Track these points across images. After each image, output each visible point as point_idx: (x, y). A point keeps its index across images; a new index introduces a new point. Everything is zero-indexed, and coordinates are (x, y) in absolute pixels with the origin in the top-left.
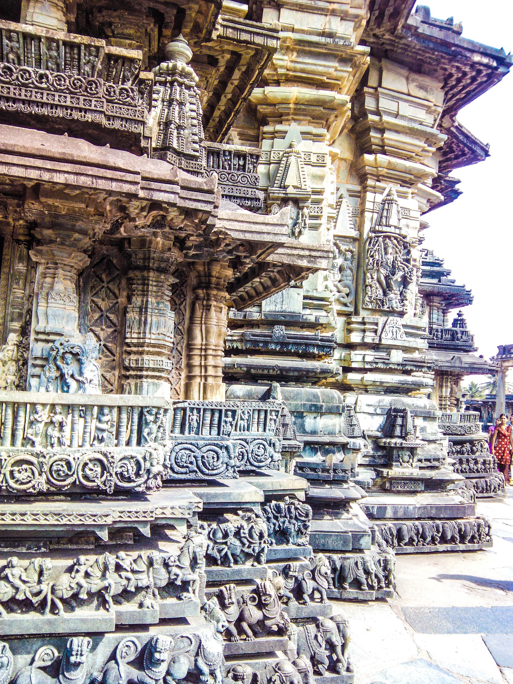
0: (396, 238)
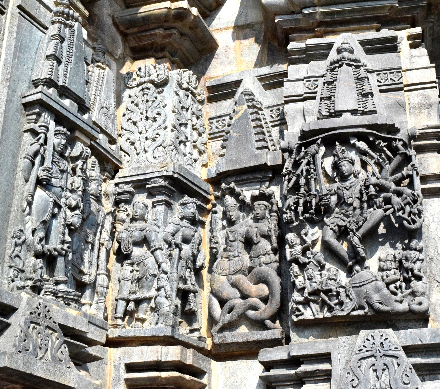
0: (361, 137)
